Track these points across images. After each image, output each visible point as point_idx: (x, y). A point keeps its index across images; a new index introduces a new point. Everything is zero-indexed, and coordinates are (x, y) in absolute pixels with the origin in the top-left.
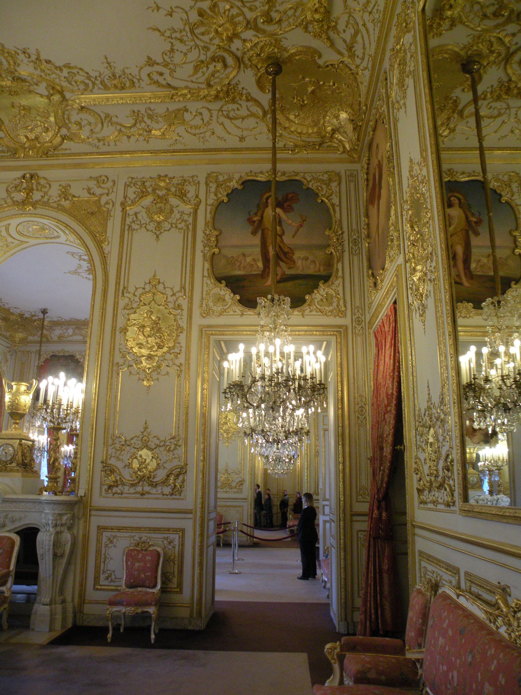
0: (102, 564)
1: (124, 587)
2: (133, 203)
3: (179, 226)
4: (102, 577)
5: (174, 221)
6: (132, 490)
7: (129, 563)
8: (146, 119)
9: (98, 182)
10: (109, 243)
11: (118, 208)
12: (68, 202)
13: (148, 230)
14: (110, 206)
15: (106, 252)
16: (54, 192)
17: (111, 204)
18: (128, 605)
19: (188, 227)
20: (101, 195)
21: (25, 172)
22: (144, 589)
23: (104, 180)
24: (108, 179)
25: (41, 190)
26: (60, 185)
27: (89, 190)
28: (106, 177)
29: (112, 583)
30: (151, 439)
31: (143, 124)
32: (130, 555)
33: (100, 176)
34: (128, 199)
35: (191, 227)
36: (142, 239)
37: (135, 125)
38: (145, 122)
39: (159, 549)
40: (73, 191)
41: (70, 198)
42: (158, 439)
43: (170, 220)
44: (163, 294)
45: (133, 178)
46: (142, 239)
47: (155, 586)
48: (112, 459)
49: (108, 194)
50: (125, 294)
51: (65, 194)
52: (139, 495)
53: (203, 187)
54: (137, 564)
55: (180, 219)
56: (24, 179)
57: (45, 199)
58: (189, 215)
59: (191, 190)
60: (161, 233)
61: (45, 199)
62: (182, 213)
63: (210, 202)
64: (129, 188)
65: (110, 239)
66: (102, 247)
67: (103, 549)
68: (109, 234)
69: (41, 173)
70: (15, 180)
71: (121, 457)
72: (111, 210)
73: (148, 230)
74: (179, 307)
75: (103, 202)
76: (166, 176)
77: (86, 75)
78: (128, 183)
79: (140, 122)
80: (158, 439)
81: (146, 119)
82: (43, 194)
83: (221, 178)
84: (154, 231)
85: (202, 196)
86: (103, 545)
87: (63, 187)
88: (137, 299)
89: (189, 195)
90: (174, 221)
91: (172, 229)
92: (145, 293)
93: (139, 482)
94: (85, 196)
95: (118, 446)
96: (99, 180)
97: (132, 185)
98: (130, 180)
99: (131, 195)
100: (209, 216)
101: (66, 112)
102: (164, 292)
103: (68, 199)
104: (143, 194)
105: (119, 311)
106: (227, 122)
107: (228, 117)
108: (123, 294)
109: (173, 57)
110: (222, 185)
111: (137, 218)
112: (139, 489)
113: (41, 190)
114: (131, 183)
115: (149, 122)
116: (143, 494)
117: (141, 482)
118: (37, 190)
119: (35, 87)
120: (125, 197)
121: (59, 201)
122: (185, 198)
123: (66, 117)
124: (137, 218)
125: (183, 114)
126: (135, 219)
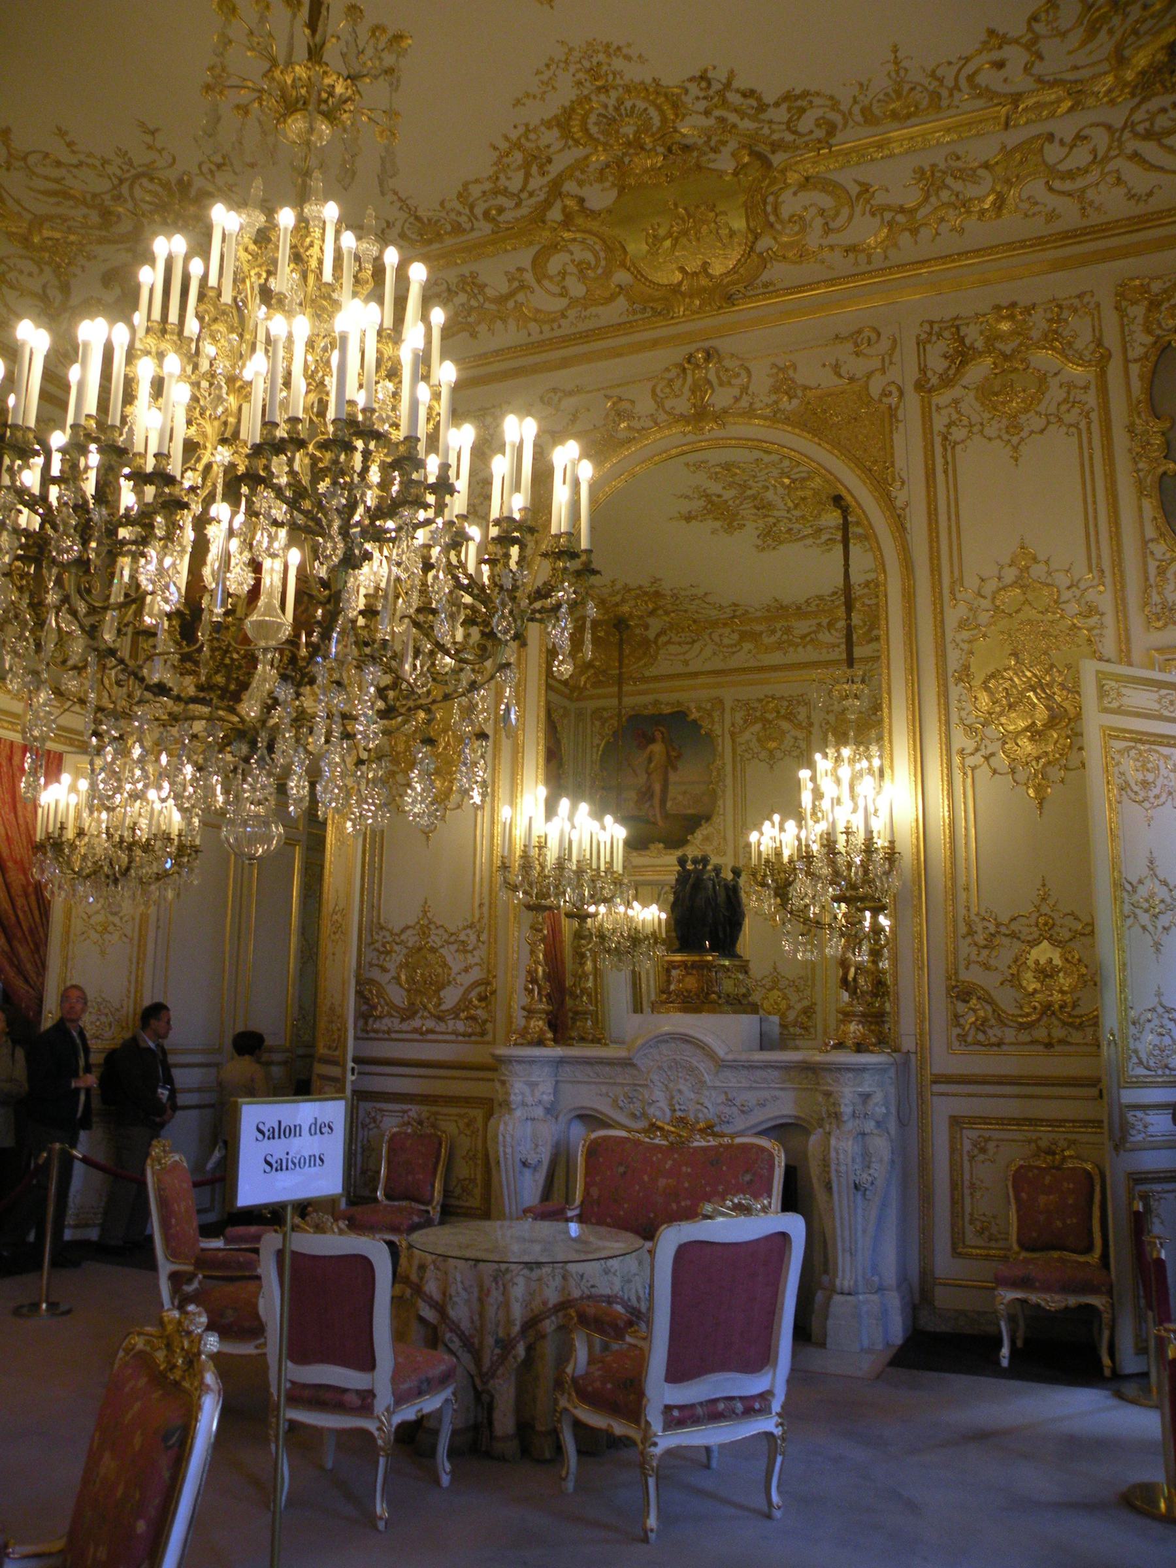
0: (968, 1200)
1: (1016, 1247)
2: (947, 381)
3: (1069, 418)
4: (970, 1230)
5: (1052, 409)
6: (1024, 1037)
7: (1024, 1195)
8: (949, 180)
9: (856, 345)
10: (903, 483)
11: (913, 400)
12: (795, 402)
13: (990, 439)
14: (894, 400)
15: (899, 503)
16: (761, 381)
17: (896, 394)
18: (1047, 1288)
19: (1087, 417)
20: (869, 375)
21: (691, 348)
22: (1067, 1255)
23: (869, 339)
24: (879, 334)
25: (730, 383)
26: (774, 365)
27: (836, 369)
28: (875, 330)
29: (993, 1244)
30: (1058, 922)
31: (945, 195)
32: (1023, 1180)
33: (859, 332)
34: (929, 374)
35: (1094, 416)
36: (981, 461)
37: (926, 199)
38: (948, 187)
39: (1089, 1167)
40: (802, 376)
41: (800, 393)
42: (1077, 919)
43: (1041, 408)
44: (1048, 585)
45: (931, 323)
46: (981, 461)
47: (1089, 1249)
48: (974, 968)
49: (883, 371)
50: (958, 596)
51: (784, 384)
52: (1041, 1048)
53: (1110, 319)
54: (1042, 1200)
55: (1066, 401)
56: (689, 362)
57: (744, 403)
58: (1086, 388)
59: (1080, 328)
60: (1022, 439)
61: (744, 403)
62: (1070, 386)
63: (1136, 352)
64: (928, 346)
65: (904, 475)
66: (888, 495)
67: (966, 1165)
68: (900, 463)
69: (724, 345)
70: (667, 370)
71: (992, 962)
72: (897, 408)
73: (990, 439)
74: (1091, 610)
75: (875, 391)
76: (1014, 305)
77: (829, 103)
78: (924, 336)
79: (939, 188)
80: (1077, 919)
81: (949, 180)
82: (736, 392)
83: (1156, 287)
84: (1006, 437)
85: (1112, 340)
86: (966, 1158)
87: (780, 369)
88: (986, 603)
89: (1079, 345)
90: (1052, 409)
91: (1051, 427)
92: (1004, 588)
93: (1039, 1020)
94: (828, 380)
95: (980, 939)
96: (858, 339)
97: (934, 338)
98: (927, 327)
99: (937, 364)
100: (1136, 385)
101: (771, 199)
102: (1049, 581)
103: (796, 396)
104: (962, 355)
105: (949, 635)
106: (1149, 150)
107: (1149, 135)
108: (952, 592)
109: (1056, 19)
110: (1159, 304)
111: (959, 412)
112: (1040, 1033)
113: (730, 383)
114: (930, 334)
115: (957, 186)
116: (1049, 1045)
117: (1045, 1018)
118: (721, 384)
119: (712, 155)
120: (923, 370)
121: (776, 402)
122: (1069, 352)
123: (769, 208)
124: (959, 412)
125: (1041, 150)
126: (955, 416)
